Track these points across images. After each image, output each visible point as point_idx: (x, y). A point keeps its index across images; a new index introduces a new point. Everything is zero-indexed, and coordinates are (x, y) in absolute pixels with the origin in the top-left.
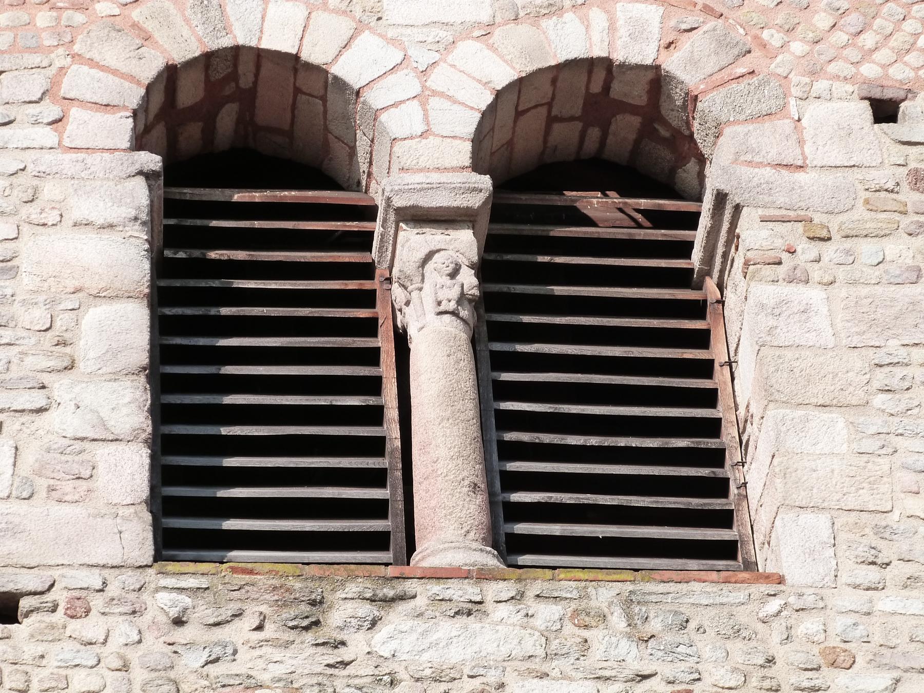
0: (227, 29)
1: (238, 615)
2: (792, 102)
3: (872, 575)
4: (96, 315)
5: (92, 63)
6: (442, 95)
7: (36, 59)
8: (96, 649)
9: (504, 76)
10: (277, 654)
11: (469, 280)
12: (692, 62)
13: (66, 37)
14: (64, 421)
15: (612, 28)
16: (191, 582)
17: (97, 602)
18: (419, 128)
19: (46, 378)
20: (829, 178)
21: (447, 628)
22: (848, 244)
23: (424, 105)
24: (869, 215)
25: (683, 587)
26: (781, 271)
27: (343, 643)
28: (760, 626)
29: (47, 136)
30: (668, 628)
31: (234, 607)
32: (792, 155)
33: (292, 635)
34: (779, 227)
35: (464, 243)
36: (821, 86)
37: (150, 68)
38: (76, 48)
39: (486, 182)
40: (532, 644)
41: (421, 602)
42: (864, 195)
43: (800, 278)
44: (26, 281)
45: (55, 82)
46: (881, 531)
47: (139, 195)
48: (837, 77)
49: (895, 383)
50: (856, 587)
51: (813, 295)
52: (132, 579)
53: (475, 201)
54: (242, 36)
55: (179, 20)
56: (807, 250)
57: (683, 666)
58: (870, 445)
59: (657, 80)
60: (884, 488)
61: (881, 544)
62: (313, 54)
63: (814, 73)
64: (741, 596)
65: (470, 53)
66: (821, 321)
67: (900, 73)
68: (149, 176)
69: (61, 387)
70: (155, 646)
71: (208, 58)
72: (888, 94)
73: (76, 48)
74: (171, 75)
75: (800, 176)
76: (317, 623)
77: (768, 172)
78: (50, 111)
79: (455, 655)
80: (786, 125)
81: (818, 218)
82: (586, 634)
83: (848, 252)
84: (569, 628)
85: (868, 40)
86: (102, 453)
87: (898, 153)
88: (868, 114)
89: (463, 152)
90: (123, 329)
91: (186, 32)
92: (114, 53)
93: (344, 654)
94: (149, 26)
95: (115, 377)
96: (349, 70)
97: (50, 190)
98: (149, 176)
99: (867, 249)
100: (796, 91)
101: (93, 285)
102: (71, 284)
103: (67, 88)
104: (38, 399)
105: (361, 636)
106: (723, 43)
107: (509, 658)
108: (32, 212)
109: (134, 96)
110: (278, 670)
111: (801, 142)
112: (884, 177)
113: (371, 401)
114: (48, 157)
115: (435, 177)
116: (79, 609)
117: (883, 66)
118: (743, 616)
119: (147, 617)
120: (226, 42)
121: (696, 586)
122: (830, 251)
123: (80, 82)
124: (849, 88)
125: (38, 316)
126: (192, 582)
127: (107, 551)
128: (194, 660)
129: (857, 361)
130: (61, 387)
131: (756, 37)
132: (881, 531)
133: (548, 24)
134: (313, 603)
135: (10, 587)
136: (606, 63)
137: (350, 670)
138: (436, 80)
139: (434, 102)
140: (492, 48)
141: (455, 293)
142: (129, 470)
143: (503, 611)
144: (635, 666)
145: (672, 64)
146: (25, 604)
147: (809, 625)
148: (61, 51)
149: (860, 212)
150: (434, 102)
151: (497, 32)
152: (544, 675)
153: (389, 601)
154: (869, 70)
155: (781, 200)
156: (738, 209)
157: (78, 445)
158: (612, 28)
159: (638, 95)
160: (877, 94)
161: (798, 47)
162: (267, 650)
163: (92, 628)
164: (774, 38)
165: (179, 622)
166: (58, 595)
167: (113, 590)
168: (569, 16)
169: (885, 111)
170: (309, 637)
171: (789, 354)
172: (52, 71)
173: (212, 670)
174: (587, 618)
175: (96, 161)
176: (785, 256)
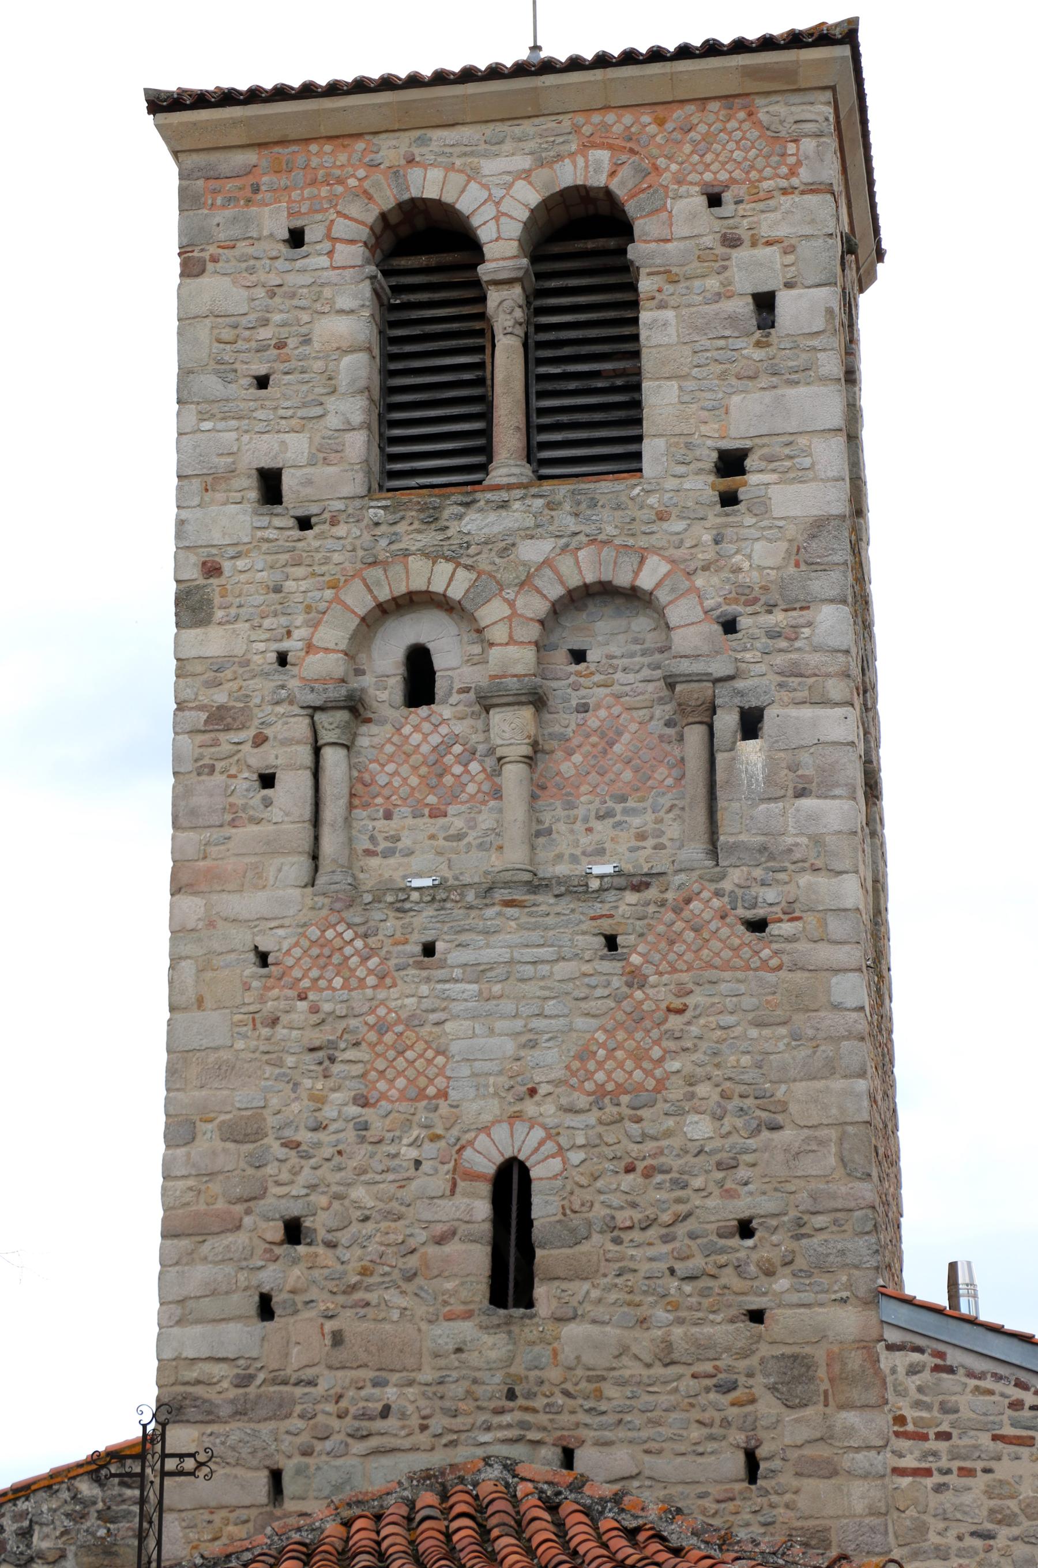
0: (408, 189)
1: (403, 518)
2: (669, 201)
3: (681, 469)
4: (347, 360)
5: (346, 217)
6: (506, 214)
7: (319, 217)
8: (342, 542)
9: (534, 198)
10: (419, 537)
11: (519, 314)
12: (622, 183)
13: (333, 200)
14: (333, 421)
15: (587, 167)
16: (384, 503)
17: (343, 517)
18: (495, 236)
19: (323, 399)
20: (682, 245)
21: (492, 516)
22: (688, 283)
23: (497, 221)
24: (699, 265)
25: (598, 485)
26: (656, 301)
27: (447, 528)
28: (630, 502)
29: (324, 261)
30: (589, 507)
31: (398, 516)
32: (665, 234)
33: (424, 527)
34: (656, 278)
35: (517, 291)
36: (683, 189)
37: (371, 216)
38: (339, 208)
39: (525, 261)
40: (530, 522)
41: (482, 503)
42: (698, 253)
43: (662, 306)
44: (317, 345)
45: (329, 229)
46: (688, 446)
47: (366, 288)
48: (691, 183)
49: (703, 361)
50: (675, 476)
51: (669, 314)
52: (358, 503)
53: (520, 274)
54: (415, 193)
55: (386, 186)
56: (669, 288)
57: (593, 527)
58: (686, 398)
59: (607, 192)
60: (692, 421)
61: (688, 452)
62: (448, 198)
63: (680, 183)
64: (622, 487)
65: (520, 184)
66: (672, 330)
67: (723, 176)
68: (373, 278)
69: (332, 404)
70: (367, 537)
71: (400, 205)
72: (716, 190)
73: (339, 208)
74: (383, 216)
75: (669, 246)
76: (436, 519)
77: (653, 245)
78: (327, 246)
79: (496, 529)
80: (664, 215)
81: (674, 270)
82: (553, 513)
83: (687, 288)
84: (546, 511)
85: (709, 157)
86: (349, 436)
87: (717, 225)
88: (706, 203)
89: (512, 248)
90: (357, 369)
91: (389, 193)
92: (354, 209)
93: (449, 533)
94: (371, 191)
95: (353, 394)
96: (464, 206)
97: (327, 292)
98: (373, 278)
99: (697, 283)
100: (671, 194)
101: (345, 345)
102: (335, 345)
103: (334, 234)
104: (317, 411)
105: (456, 523)
106: (637, 169)
107: (519, 529)
108: (318, 306)
109: (364, 233)
110: (419, 545)
111: (671, 225)
112: (708, 241)
113: (480, 373)
114: (325, 273)
115: (502, 264)
116: (334, 522)
117: (715, 173)
118: (623, 498)
119: (365, 522)
120: (406, 197)
121: (603, 484)
122: (681, 287)
123: (342, 228)
124: (697, 189)
125: (318, 365)
126: (384, 503)
127: (347, 490)
128: (383, 543)
129: (687, 350)
130: (332, 404)
131: (654, 164)
132: (688, 446)
133: (556, 166)
134: (434, 508)
135: (306, 513)
136: (584, 187)
137: (451, 542)
138: (503, 208)
139: (503, 219)
140: (530, 183)
141: (510, 323)
142: (358, 445)
143: (517, 505)
144: (574, 528)
145: (614, 186)
146: (313, 520)
147: (652, 500)
148: (332, 211)
149: (696, 264)
150: (503, 219)
151: (534, 174)
152: (532, 537)
153: (467, 505)
154: (708, 177)
155: (658, 261)
156: (638, 268)
157: (336, 434)
158: (587, 167)
159: (601, 195)
160: (710, 190)
161: (674, 167)
162: (414, 535)
163: (341, 530)
164: (661, 162)
165: (377, 524)
166: (326, 515)
167: (350, 511)
168: (567, 161)
169: (714, 200)
170: (433, 526)
171: (654, 350)
172: (327, 223)
173: (394, 547)
174: (552, 506)
175: (348, 273)
176: (657, 294)
